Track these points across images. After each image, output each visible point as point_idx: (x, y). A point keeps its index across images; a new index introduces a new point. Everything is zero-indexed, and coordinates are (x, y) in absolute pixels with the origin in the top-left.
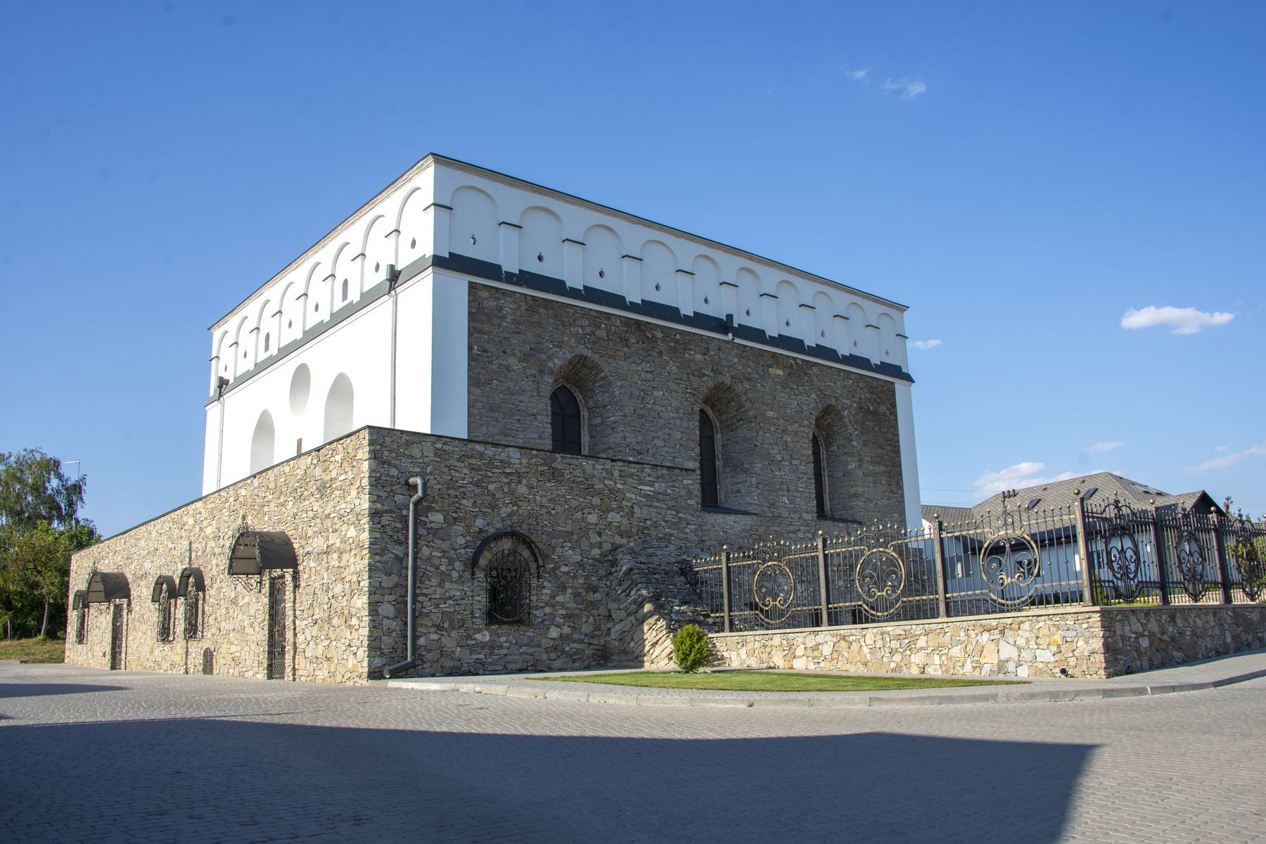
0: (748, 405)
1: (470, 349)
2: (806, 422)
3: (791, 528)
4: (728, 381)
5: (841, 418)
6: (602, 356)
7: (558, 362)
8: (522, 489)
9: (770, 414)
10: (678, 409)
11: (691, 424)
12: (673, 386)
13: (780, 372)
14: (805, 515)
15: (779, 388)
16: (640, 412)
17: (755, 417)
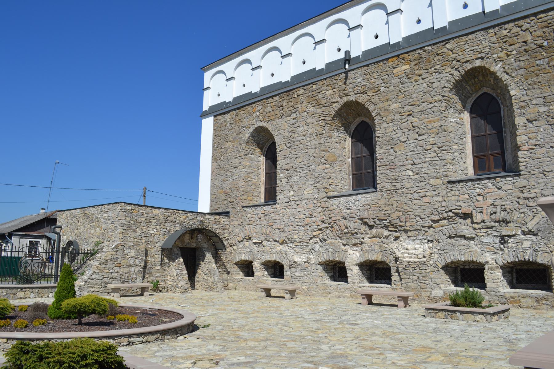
0: (371, 108)
1: (213, 146)
2: (440, 97)
3: (416, 196)
4: (352, 98)
5: (493, 74)
6: (268, 122)
7: (247, 135)
8: (79, 224)
9: (394, 106)
10: (313, 134)
11: (322, 141)
12: (309, 120)
13: (406, 67)
14: (432, 182)
15: (405, 80)
16: (288, 145)
17: (378, 114)
